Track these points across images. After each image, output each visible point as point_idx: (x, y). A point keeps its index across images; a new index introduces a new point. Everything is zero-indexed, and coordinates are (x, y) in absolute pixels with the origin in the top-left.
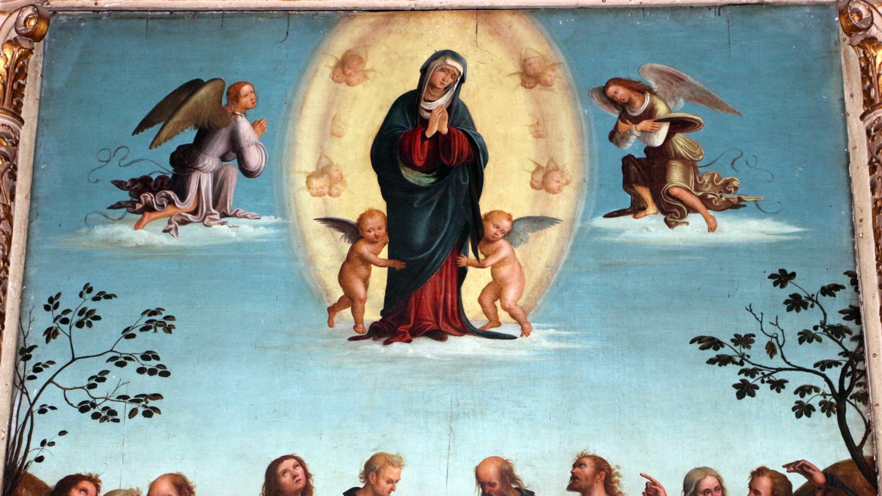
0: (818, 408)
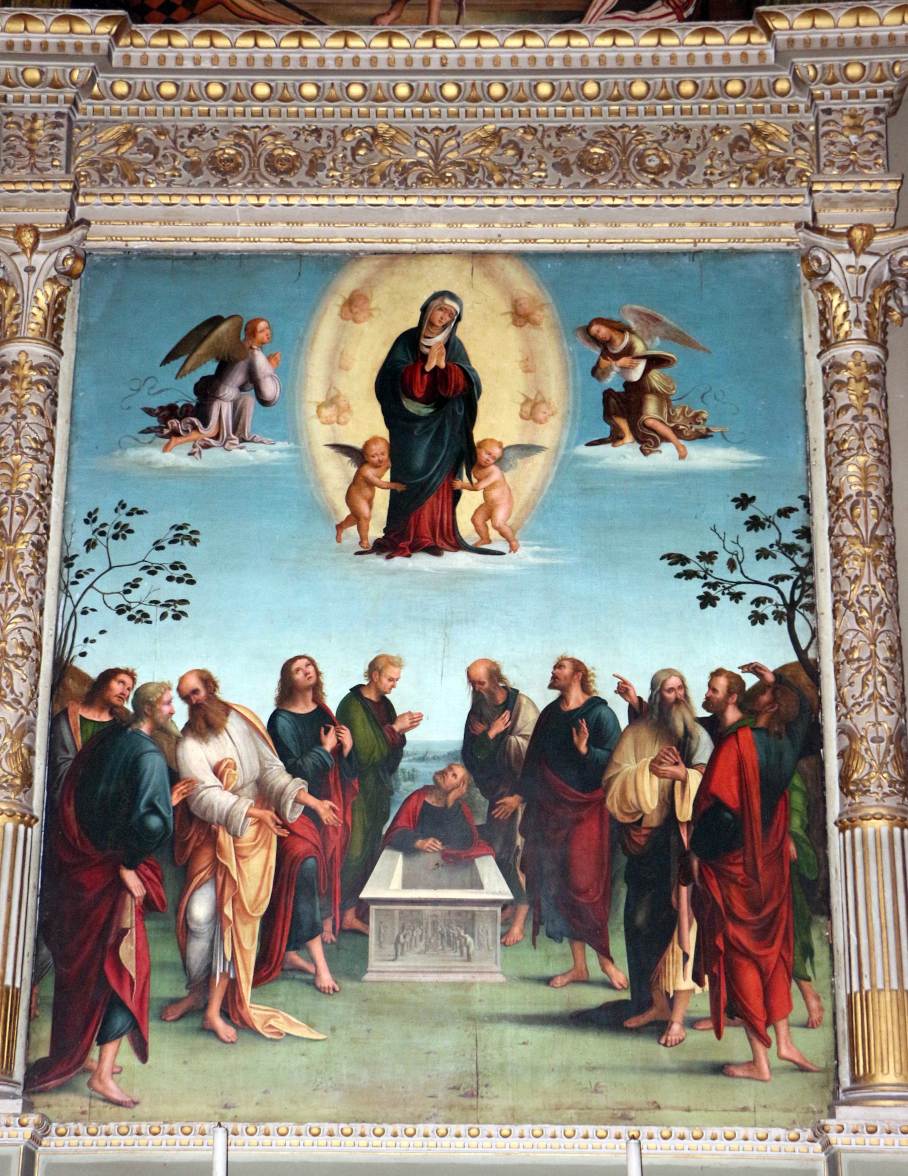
0: (771, 617)
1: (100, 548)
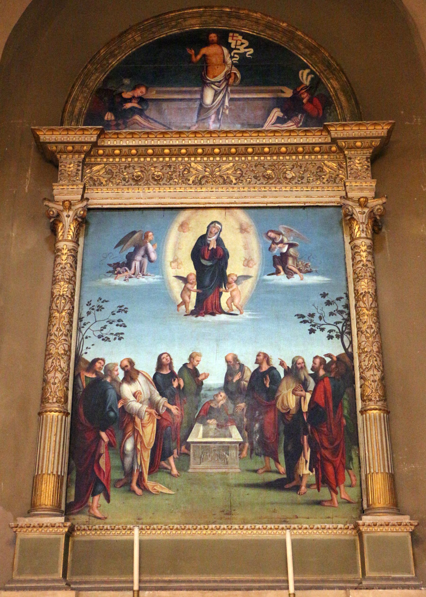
0: (335, 336)
1: (92, 314)
